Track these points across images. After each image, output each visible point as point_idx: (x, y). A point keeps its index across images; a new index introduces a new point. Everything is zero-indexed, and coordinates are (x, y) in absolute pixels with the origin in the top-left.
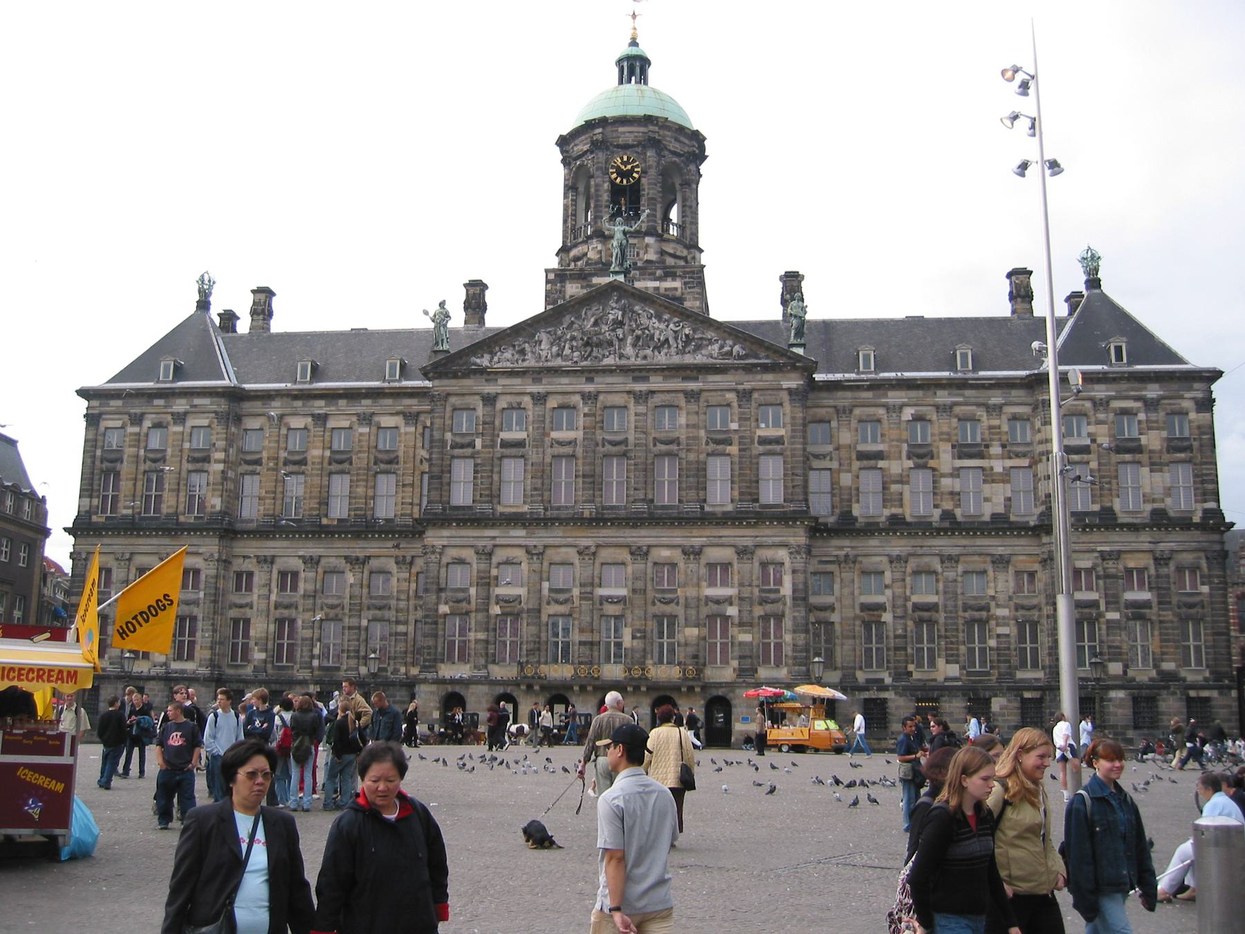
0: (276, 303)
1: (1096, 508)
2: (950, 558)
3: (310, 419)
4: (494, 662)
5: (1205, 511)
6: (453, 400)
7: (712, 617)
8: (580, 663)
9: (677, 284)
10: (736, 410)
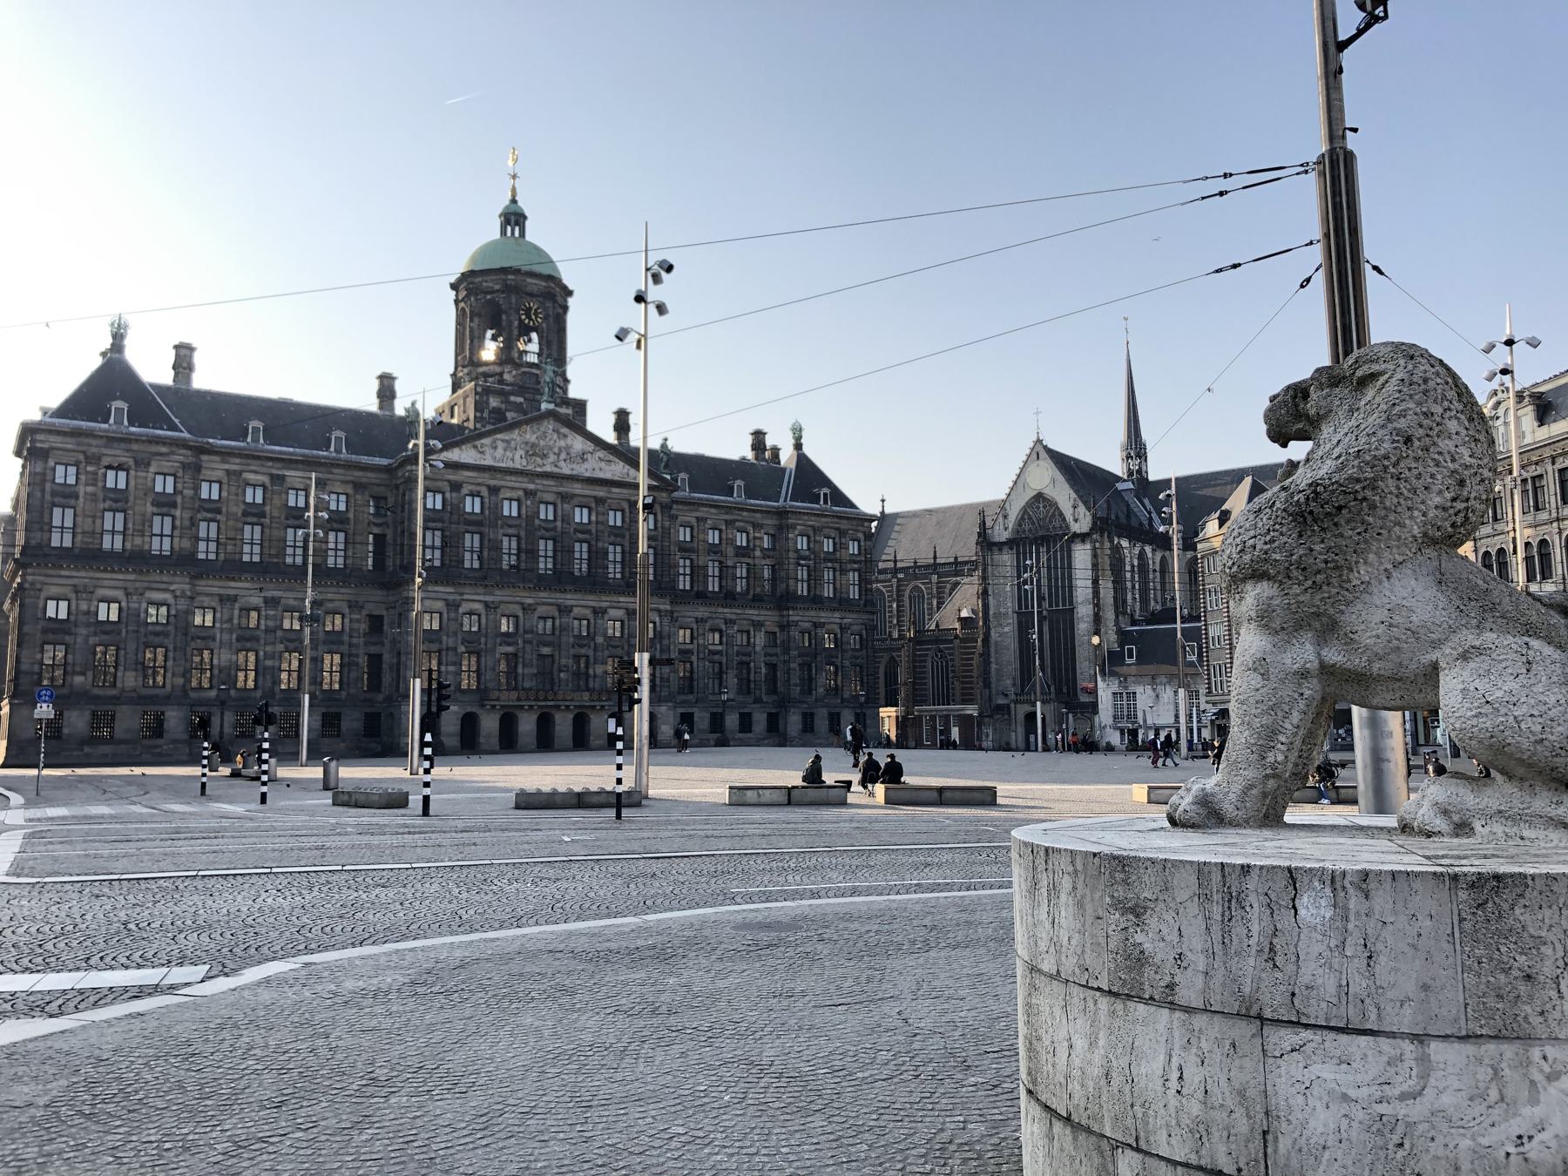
0: (197, 359)
9: (570, 411)
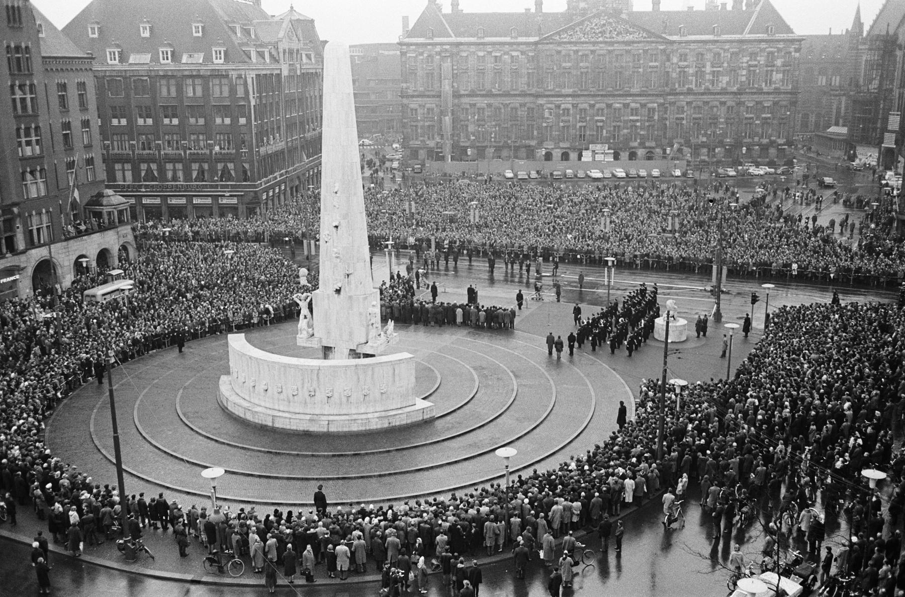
7: (632, 126)
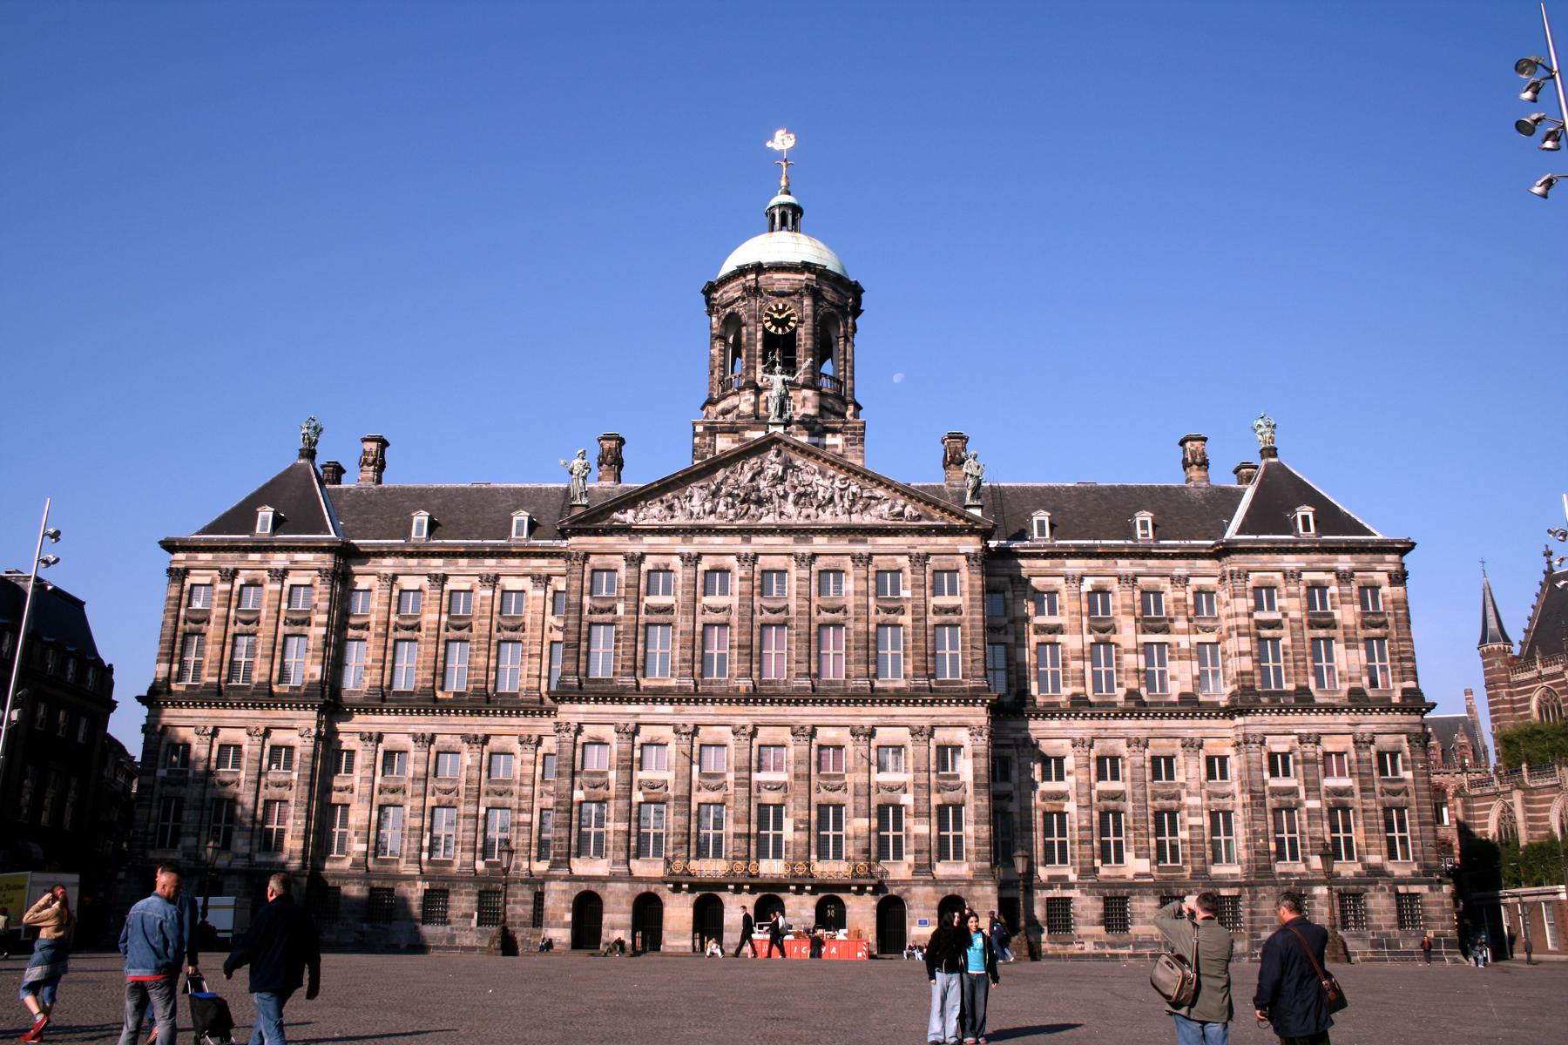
1: (1291, 687)
2: (1138, 741)
3: (426, 579)
4: (637, 857)
5: (1404, 691)
6: (592, 559)
7: (882, 810)
8: (735, 858)
10: (909, 576)
